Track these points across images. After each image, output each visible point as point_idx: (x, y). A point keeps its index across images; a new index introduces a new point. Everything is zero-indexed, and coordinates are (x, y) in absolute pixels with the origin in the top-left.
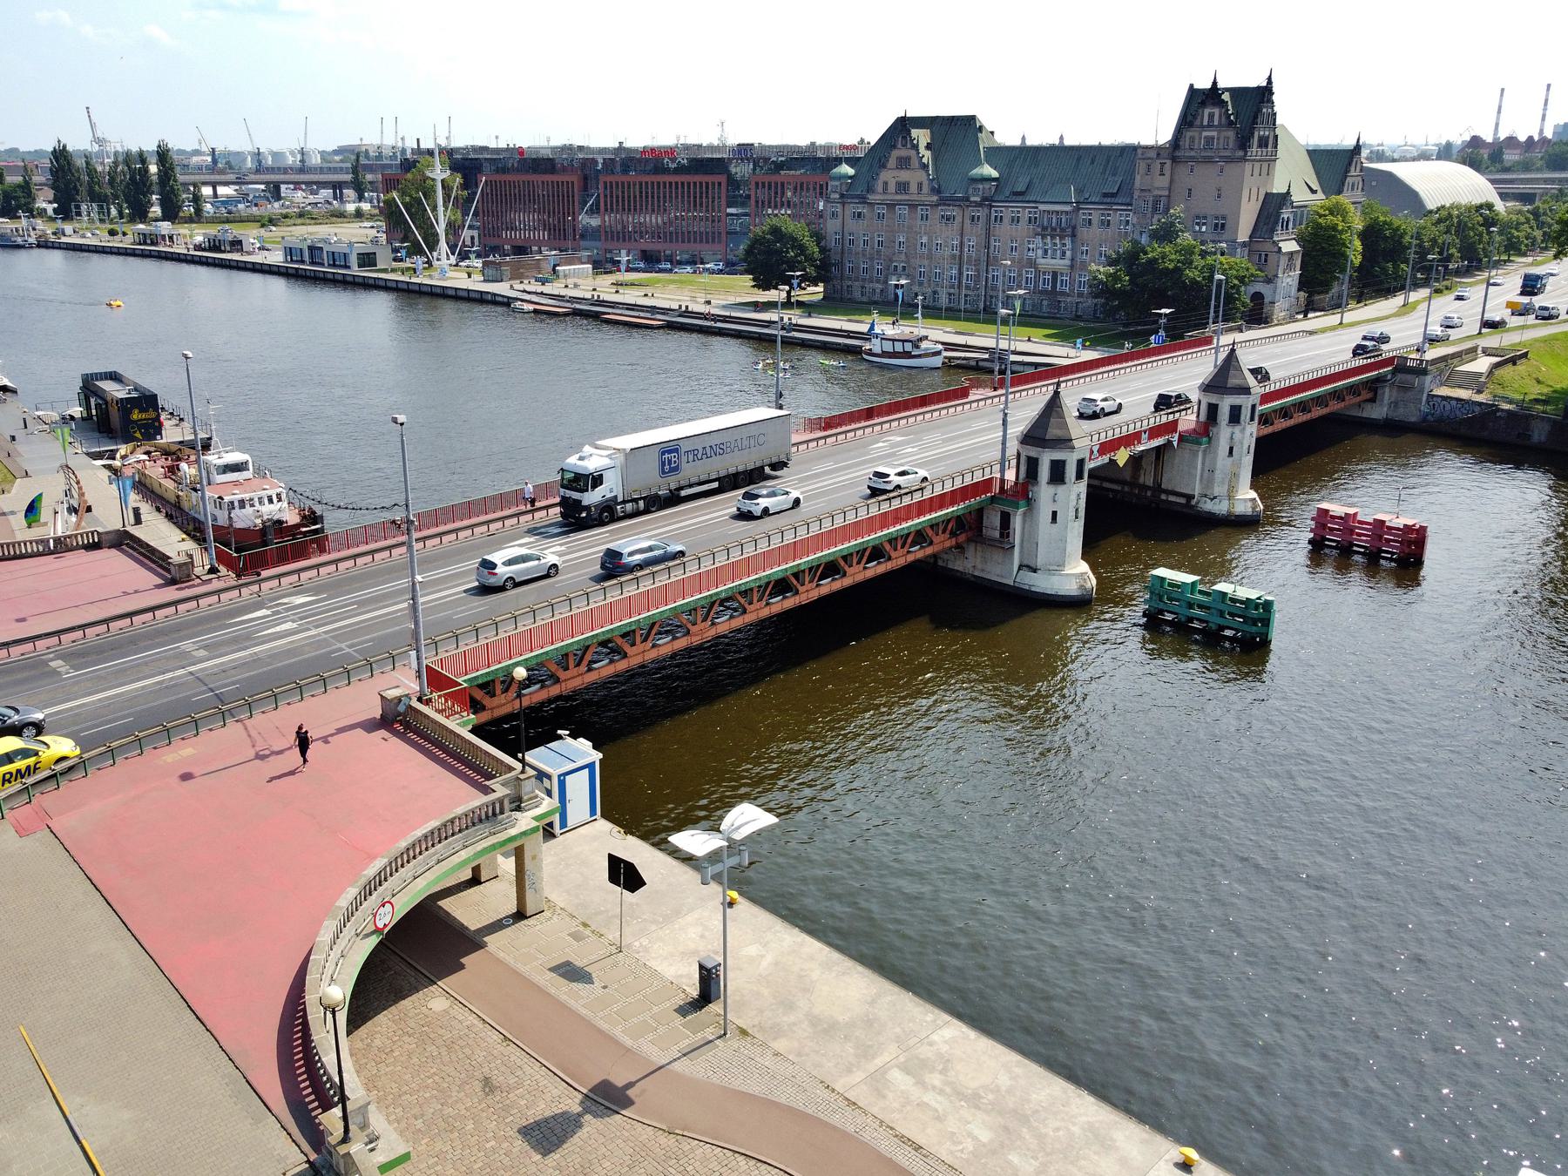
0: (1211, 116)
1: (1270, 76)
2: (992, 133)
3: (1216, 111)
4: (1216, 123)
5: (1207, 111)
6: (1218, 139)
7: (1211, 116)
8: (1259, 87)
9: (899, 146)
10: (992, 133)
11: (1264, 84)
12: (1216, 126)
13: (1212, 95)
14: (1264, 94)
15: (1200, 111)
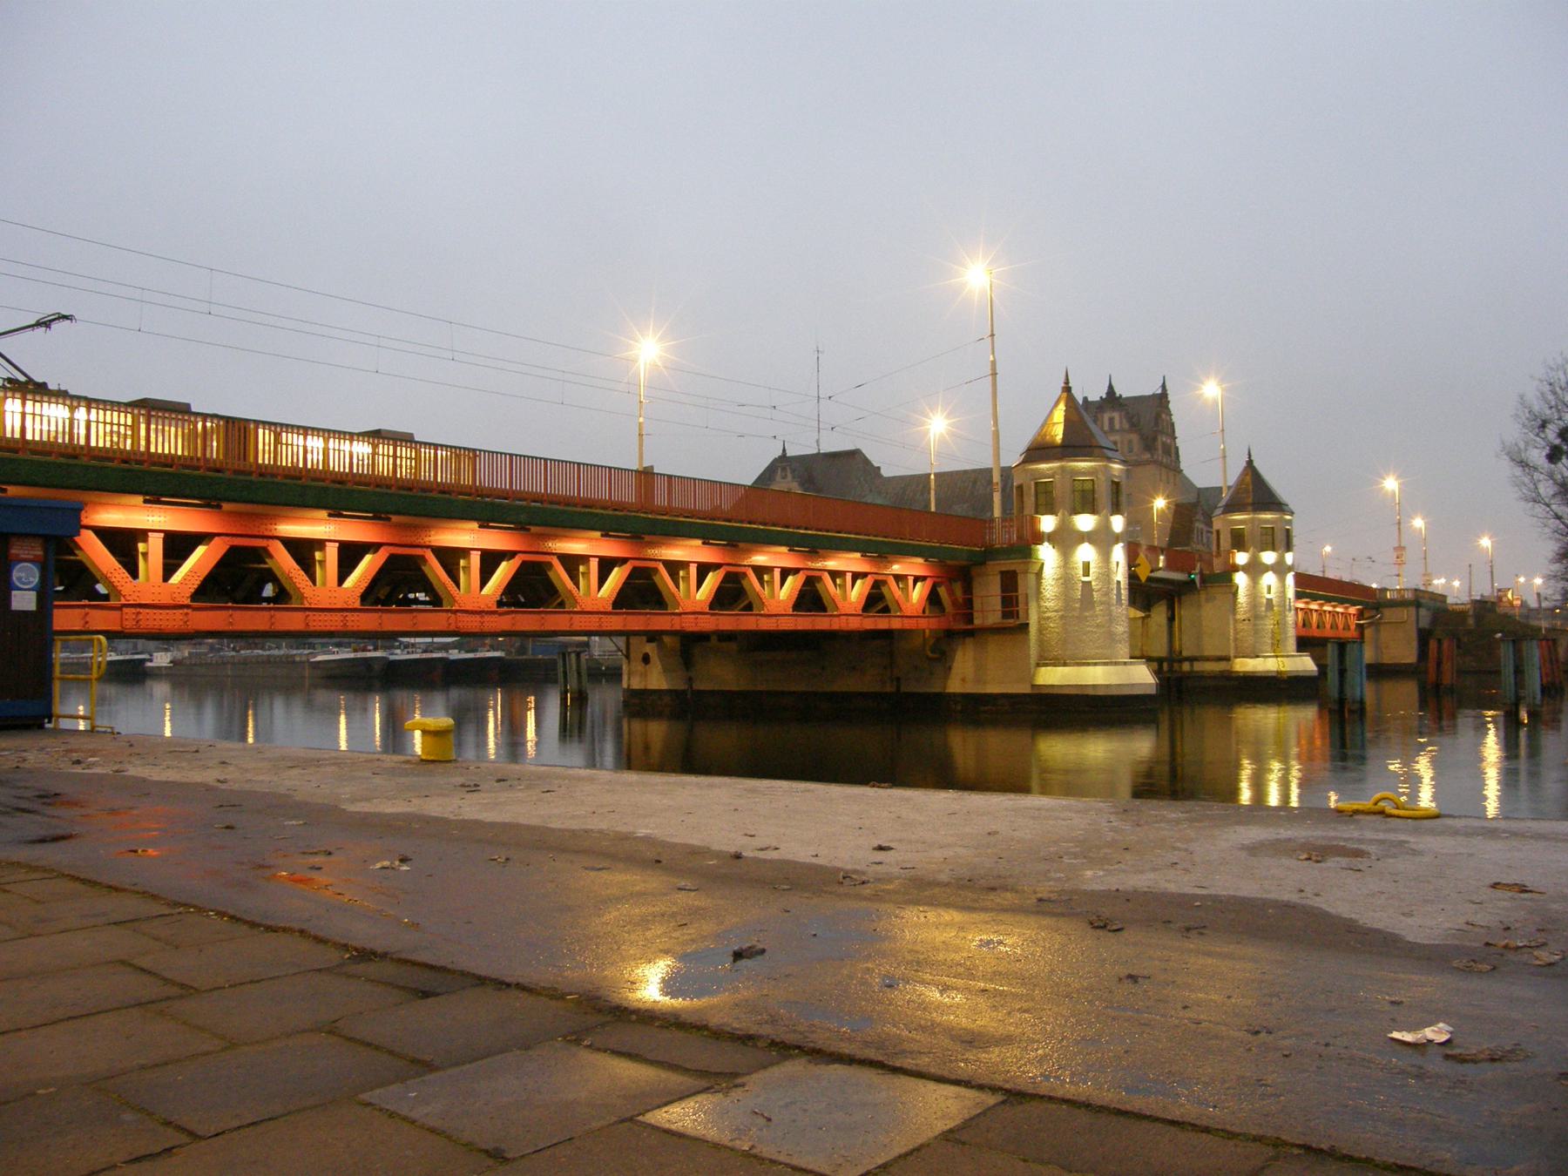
0: (1111, 420)
1: (1164, 383)
2: (879, 468)
3: (1116, 415)
4: (1117, 426)
5: (1106, 416)
6: (1122, 442)
7: (1111, 420)
8: (1154, 395)
9: (778, 478)
10: (879, 468)
11: (1159, 391)
12: (1118, 431)
13: (1112, 399)
14: (1161, 400)
15: (1099, 416)
